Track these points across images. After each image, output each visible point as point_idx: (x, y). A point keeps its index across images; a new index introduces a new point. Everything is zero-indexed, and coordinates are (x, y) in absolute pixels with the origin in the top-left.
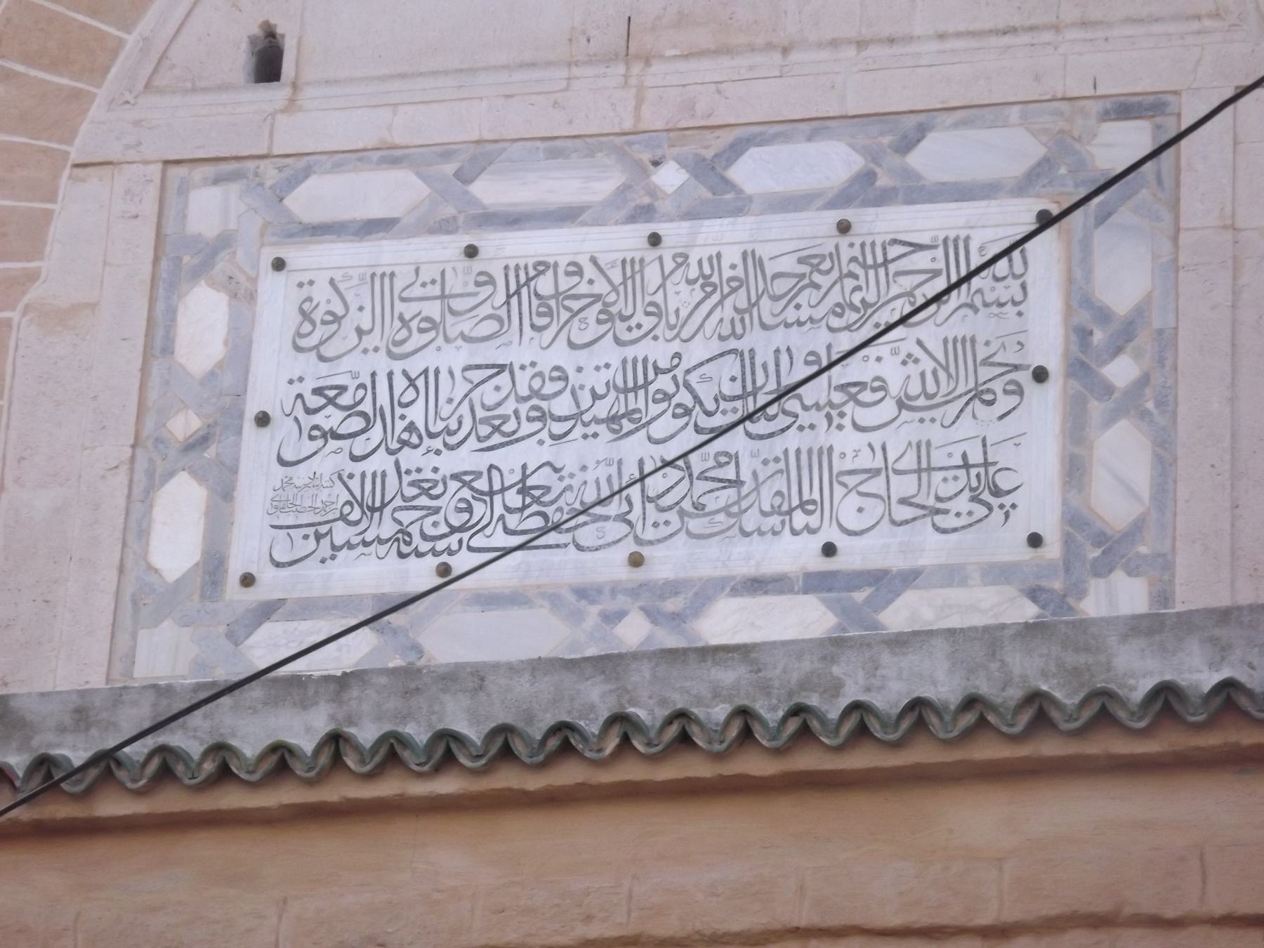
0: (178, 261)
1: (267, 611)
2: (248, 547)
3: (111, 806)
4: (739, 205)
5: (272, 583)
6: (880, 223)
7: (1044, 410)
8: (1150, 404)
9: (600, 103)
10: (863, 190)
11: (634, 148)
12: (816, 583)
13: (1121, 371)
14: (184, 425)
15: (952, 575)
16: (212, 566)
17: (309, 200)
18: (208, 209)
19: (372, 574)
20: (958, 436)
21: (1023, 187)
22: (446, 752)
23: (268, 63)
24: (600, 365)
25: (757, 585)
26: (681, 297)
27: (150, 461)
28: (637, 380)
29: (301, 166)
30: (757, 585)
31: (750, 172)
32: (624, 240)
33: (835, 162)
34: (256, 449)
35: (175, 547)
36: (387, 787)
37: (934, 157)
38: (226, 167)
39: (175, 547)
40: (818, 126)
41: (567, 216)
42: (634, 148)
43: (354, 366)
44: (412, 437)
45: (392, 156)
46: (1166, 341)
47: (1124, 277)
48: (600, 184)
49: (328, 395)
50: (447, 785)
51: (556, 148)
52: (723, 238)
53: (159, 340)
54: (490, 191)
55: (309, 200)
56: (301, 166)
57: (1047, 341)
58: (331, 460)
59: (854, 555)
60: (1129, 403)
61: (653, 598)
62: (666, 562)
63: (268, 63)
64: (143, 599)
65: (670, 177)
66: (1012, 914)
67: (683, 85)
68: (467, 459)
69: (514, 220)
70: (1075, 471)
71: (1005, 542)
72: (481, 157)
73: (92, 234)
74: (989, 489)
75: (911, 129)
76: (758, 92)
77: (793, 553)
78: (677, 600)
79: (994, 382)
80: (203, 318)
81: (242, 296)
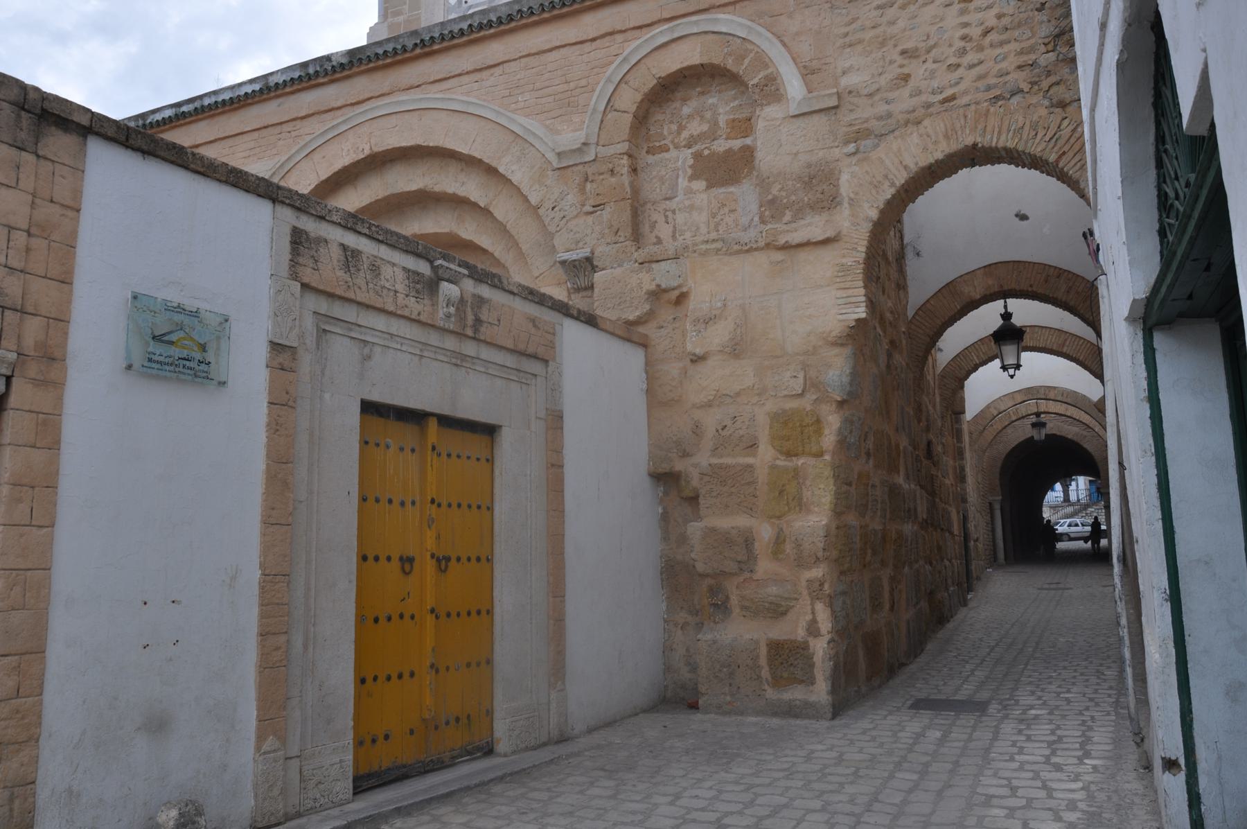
1: (470, 7)
3: (436, 47)
22: (490, 24)
36: (482, 34)
50: (492, 31)
66: (595, 35)
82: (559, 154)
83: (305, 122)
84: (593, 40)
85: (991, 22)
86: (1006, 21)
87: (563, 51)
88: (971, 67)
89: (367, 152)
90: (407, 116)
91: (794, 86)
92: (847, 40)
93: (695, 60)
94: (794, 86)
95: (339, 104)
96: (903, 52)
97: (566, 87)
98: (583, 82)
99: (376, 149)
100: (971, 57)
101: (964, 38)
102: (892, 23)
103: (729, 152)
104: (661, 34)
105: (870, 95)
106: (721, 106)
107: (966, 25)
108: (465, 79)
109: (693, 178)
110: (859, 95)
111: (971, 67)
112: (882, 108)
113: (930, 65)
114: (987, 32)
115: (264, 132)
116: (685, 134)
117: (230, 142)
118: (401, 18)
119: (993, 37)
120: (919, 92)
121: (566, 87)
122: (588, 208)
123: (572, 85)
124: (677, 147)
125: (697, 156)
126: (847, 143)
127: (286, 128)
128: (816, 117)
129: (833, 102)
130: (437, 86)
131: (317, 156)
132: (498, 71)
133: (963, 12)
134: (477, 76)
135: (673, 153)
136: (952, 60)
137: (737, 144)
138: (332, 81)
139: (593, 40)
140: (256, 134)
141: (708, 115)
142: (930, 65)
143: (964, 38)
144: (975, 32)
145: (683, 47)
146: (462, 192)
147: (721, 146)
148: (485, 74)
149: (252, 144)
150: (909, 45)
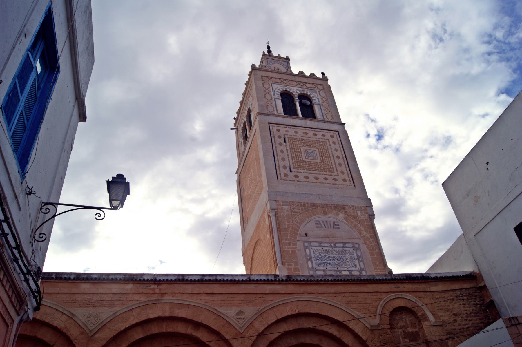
0: (306, 248)
1: (317, 270)
2: (315, 266)
4: (336, 247)
5: (317, 268)
6: (345, 249)
7: (357, 261)
8: (362, 261)
9: (327, 240)
10: (343, 247)
11: (330, 243)
12: (348, 271)
13: (360, 259)
14: (309, 258)
15: (355, 271)
16: (313, 267)
17: (312, 244)
18: (306, 244)
19: (322, 268)
20: (353, 262)
21: (352, 247)
23: (306, 235)
24: (332, 256)
25: (344, 270)
26: (335, 252)
27: (307, 260)
28: (334, 257)
29: (311, 242)
30: (344, 270)
31: (337, 245)
32: (331, 248)
33: (341, 245)
34: (313, 260)
35: (310, 266)
37: (347, 245)
38: (307, 242)
39: (310, 266)
40: (340, 243)
41: (327, 247)
42: (330, 243)
43: (318, 255)
44: (322, 260)
45: (316, 242)
46: (362, 258)
47: (359, 254)
48: (329, 245)
49: (317, 257)
51: (326, 242)
52: (336, 249)
53: (306, 252)
54: (322, 245)
55: (312, 244)
56: (311, 242)
57: (356, 257)
58: (317, 261)
59: (349, 269)
60: (361, 261)
61: (339, 271)
62: (339, 269)
63: (306, 235)
64: (309, 269)
65: (332, 245)
67: (332, 240)
68: (326, 261)
69: (324, 247)
70: (360, 265)
71: (357, 269)
72: (321, 243)
73: (299, 245)
74: (355, 266)
75: (345, 244)
76: (336, 241)
77: (346, 269)
78: (340, 271)
79: (353, 259)
80: (308, 251)
81: (310, 250)
82: (372, 326)
83: (267, 295)
84: (372, 293)
85: (471, 311)
86: (474, 311)
87: (363, 294)
88: (470, 320)
89: (297, 312)
90: (311, 302)
91: (432, 318)
92: (439, 308)
93: (403, 305)
94: (432, 318)
95: (283, 292)
96: (454, 314)
97: (366, 305)
98: (371, 305)
99: (300, 312)
100: (469, 318)
101: (466, 313)
102: (449, 306)
103: (412, 332)
104: (393, 296)
105: (449, 323)
106: (408, 319)
107: (466, 310)
108: (331, 295)
109: (405, 338)
110: (446, 323)
111: (470, 320)
112: (453, 327)
113: (460, 318)
114: (471, 313)
115: (248, 295)
116: (399, 325)
117: (232, 296)
118: (291, 267)
119: (472, 314)
120: (460, 325)
121: (366, 305)
122: (382, 344)
123: (368, 305)
124: (398, 328)
125: (404, 332)
126: (447, 335)
127: (258, 296)
128: (438, 327)
129: (441, 324)
130: (321, 295)
131: (275, 309)
132: (342, 295)
133: (464, 307)
134: (335, 295)
135: (396, 330)
136: (465, 318)
137: (414, 330)
138: (279, 284)
139: (372, 293)
140: (245, 295)
141: (404, 320)
142: (460, 318)
143: (466, 313)
144: (469, 312)
145: (398, 301)
146: (330, 331)
147: (410, 330)
148: (338, 295)
149: (243, 299)
150: (455, 312)
